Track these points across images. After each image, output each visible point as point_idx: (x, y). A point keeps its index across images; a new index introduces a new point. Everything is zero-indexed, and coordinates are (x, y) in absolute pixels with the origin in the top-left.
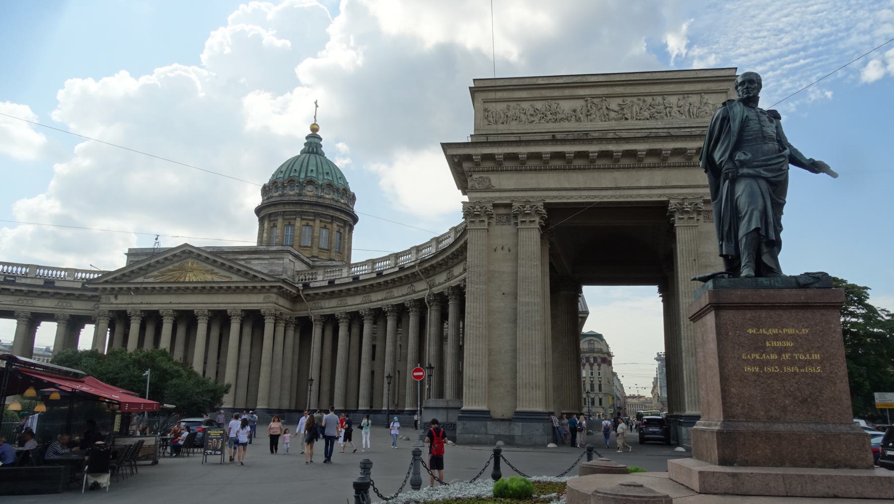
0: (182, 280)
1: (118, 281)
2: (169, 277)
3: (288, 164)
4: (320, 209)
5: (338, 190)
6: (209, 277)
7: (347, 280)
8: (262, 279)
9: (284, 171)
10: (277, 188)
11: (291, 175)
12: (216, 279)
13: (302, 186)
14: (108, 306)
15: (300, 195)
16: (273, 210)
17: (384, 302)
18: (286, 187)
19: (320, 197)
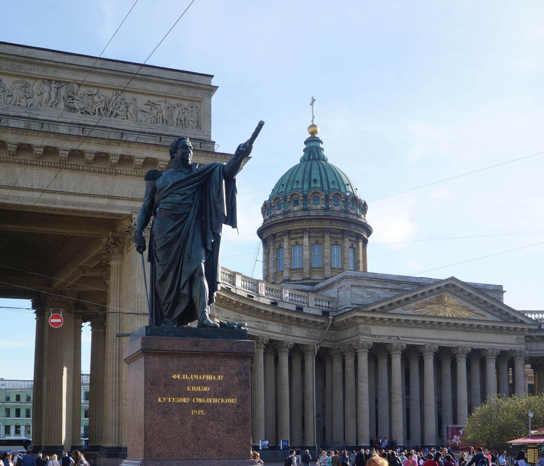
1: (381, 310)
2: (429, 311)
4: (360, 229)
6: (466, 314)
9: (319, 180)
12: (472, 317)
16: (316, 225)
19: (360, 217)
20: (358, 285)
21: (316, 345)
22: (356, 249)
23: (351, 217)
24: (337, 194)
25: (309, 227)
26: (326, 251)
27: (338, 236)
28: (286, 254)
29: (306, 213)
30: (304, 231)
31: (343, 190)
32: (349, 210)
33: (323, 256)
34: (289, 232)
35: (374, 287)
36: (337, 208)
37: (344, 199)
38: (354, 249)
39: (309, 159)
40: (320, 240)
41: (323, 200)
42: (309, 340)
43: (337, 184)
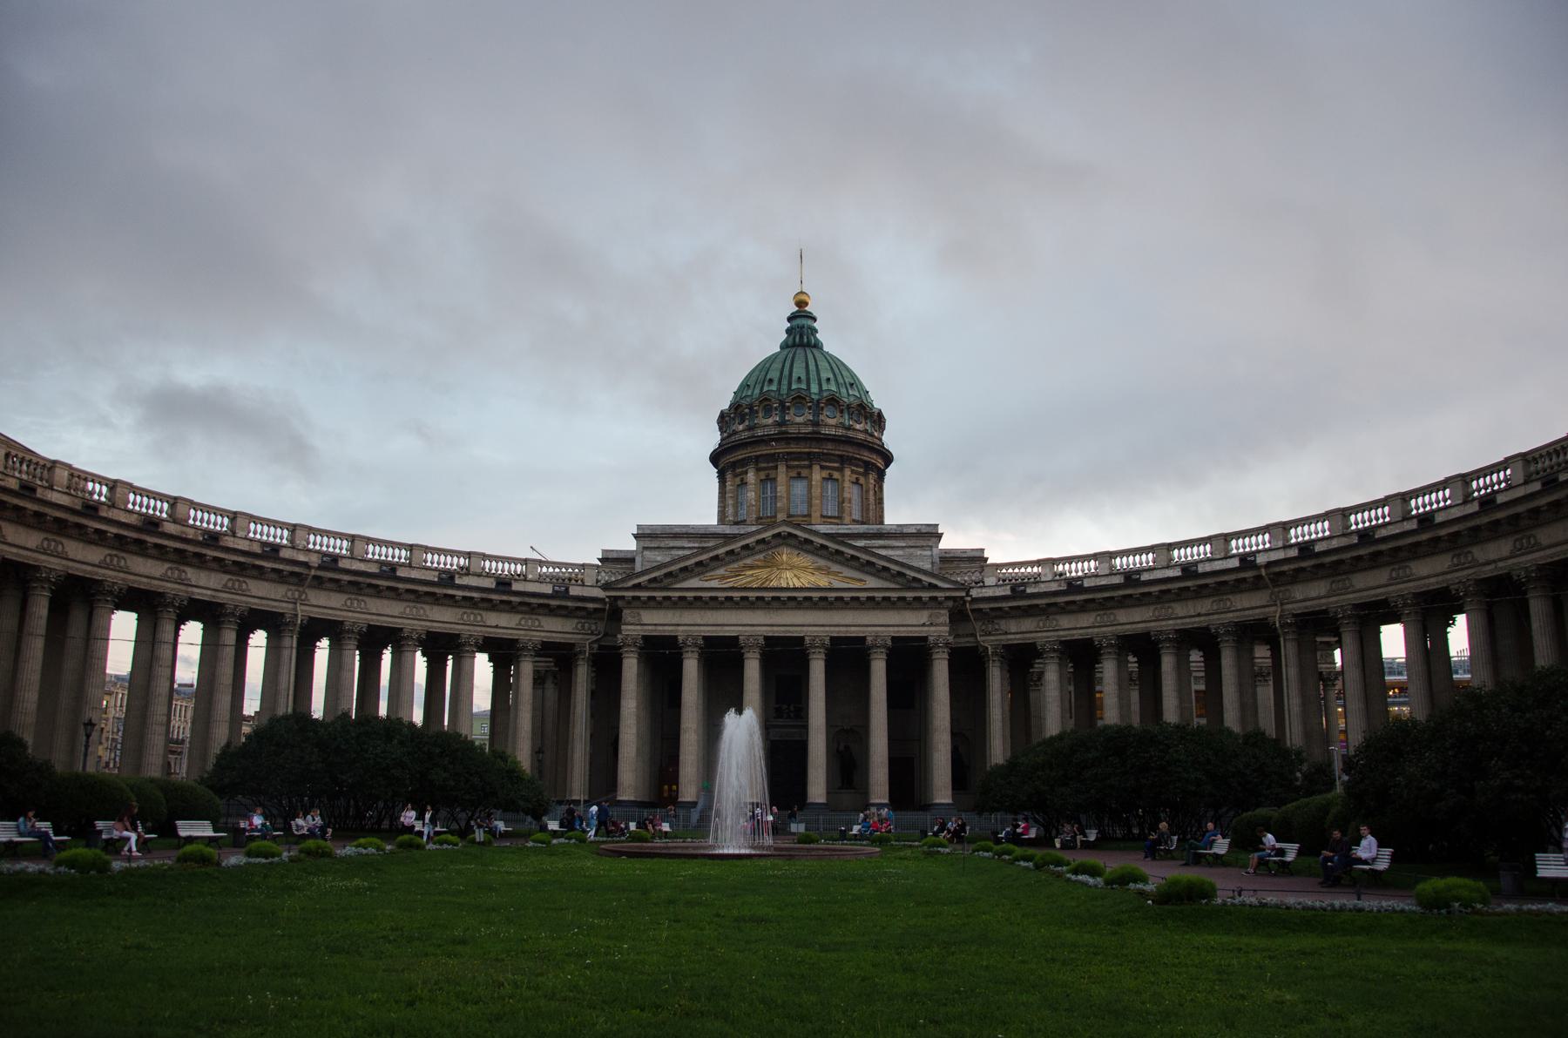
0: (774, 584)
2: (749, 579)
3: (777, 365)
5: (872, 414)
6: (823, 582)
7: (1054, 587)
8: (930, 584)
10: (768, 411)
11: (794, 387)
12: (837, 584)
13: (817, 407)
14: (639, 627)
15: (816, 424)
16: (764, 450)
17: (1153, 624)
18: (789, 408)
19: (849, 428)
20: (656, 546)
21: (589, 644)
22: (840, 481)
24: (799, 397)
25: (755, 454)
26: (779, 488)
27: (803, 463)
31: (814, 388)
32: (822, 420)
33: (776, 497)
34: (734, 465)
35: (683, 548)
36: (799, 420)
37: (809, 404)
38: (837, 480)
40: (772, 474)
41: (776, 409)
42: (580, 636)
43: (805, 382)
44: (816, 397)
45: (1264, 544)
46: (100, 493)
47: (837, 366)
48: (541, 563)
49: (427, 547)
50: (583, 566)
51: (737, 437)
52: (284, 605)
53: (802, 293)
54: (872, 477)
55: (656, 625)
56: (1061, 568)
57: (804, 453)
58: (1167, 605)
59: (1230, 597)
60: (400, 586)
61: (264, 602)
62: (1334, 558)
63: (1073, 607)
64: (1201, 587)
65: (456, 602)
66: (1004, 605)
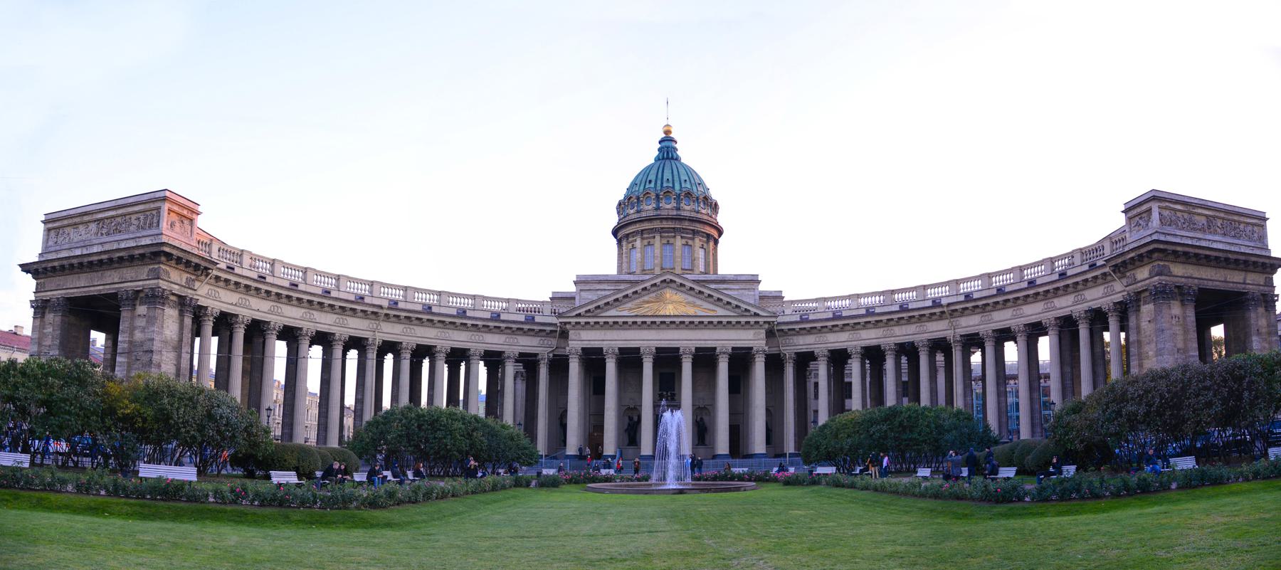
1: (588, 314)
3: (654, 172)
4: (698, 225)
5: (711, 203)
14: (579, 342)
15: (678, 209)
17: (882, 340)
18: (662, 199)
19: (698, 212)
23: (683, 213)
26: (656, 250)
27: (670, 234)
28: (637, 255)
29: (638, 215)
30: (634, 234)
31: (677, 187)
33: (654, 256)
34: (627, 236)
38: (691, 246)
39: (663, 159)
40: (652, 241)
42: (541, 349)
44: (678, 192)
45: (946, 292)
46: (264, 268)
47: (689, 172)
48: (518, 301)
49: (449, 293)
50: (543, 303)
51: (630, 217)
52: (368, 333)
53: (668, 125)
54: (712, 244)
55: (589, 340)
56: (829, 303)
57: (671, 228)
58: (890, 328)
59: (926, 324)
60: (436, 318)
61: (357, 331)
62: (984, 302)
63: (837, 329)
64: (910, 317)
65: (468, 328)
66: (797, 327)
